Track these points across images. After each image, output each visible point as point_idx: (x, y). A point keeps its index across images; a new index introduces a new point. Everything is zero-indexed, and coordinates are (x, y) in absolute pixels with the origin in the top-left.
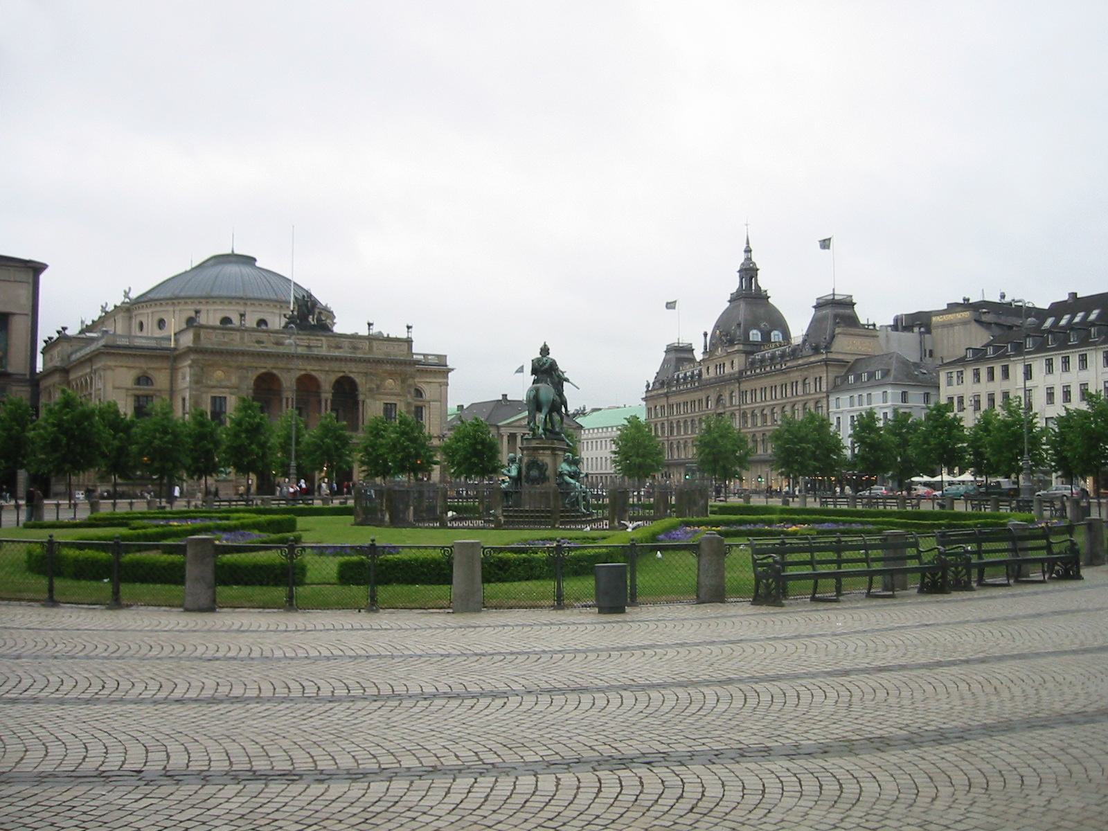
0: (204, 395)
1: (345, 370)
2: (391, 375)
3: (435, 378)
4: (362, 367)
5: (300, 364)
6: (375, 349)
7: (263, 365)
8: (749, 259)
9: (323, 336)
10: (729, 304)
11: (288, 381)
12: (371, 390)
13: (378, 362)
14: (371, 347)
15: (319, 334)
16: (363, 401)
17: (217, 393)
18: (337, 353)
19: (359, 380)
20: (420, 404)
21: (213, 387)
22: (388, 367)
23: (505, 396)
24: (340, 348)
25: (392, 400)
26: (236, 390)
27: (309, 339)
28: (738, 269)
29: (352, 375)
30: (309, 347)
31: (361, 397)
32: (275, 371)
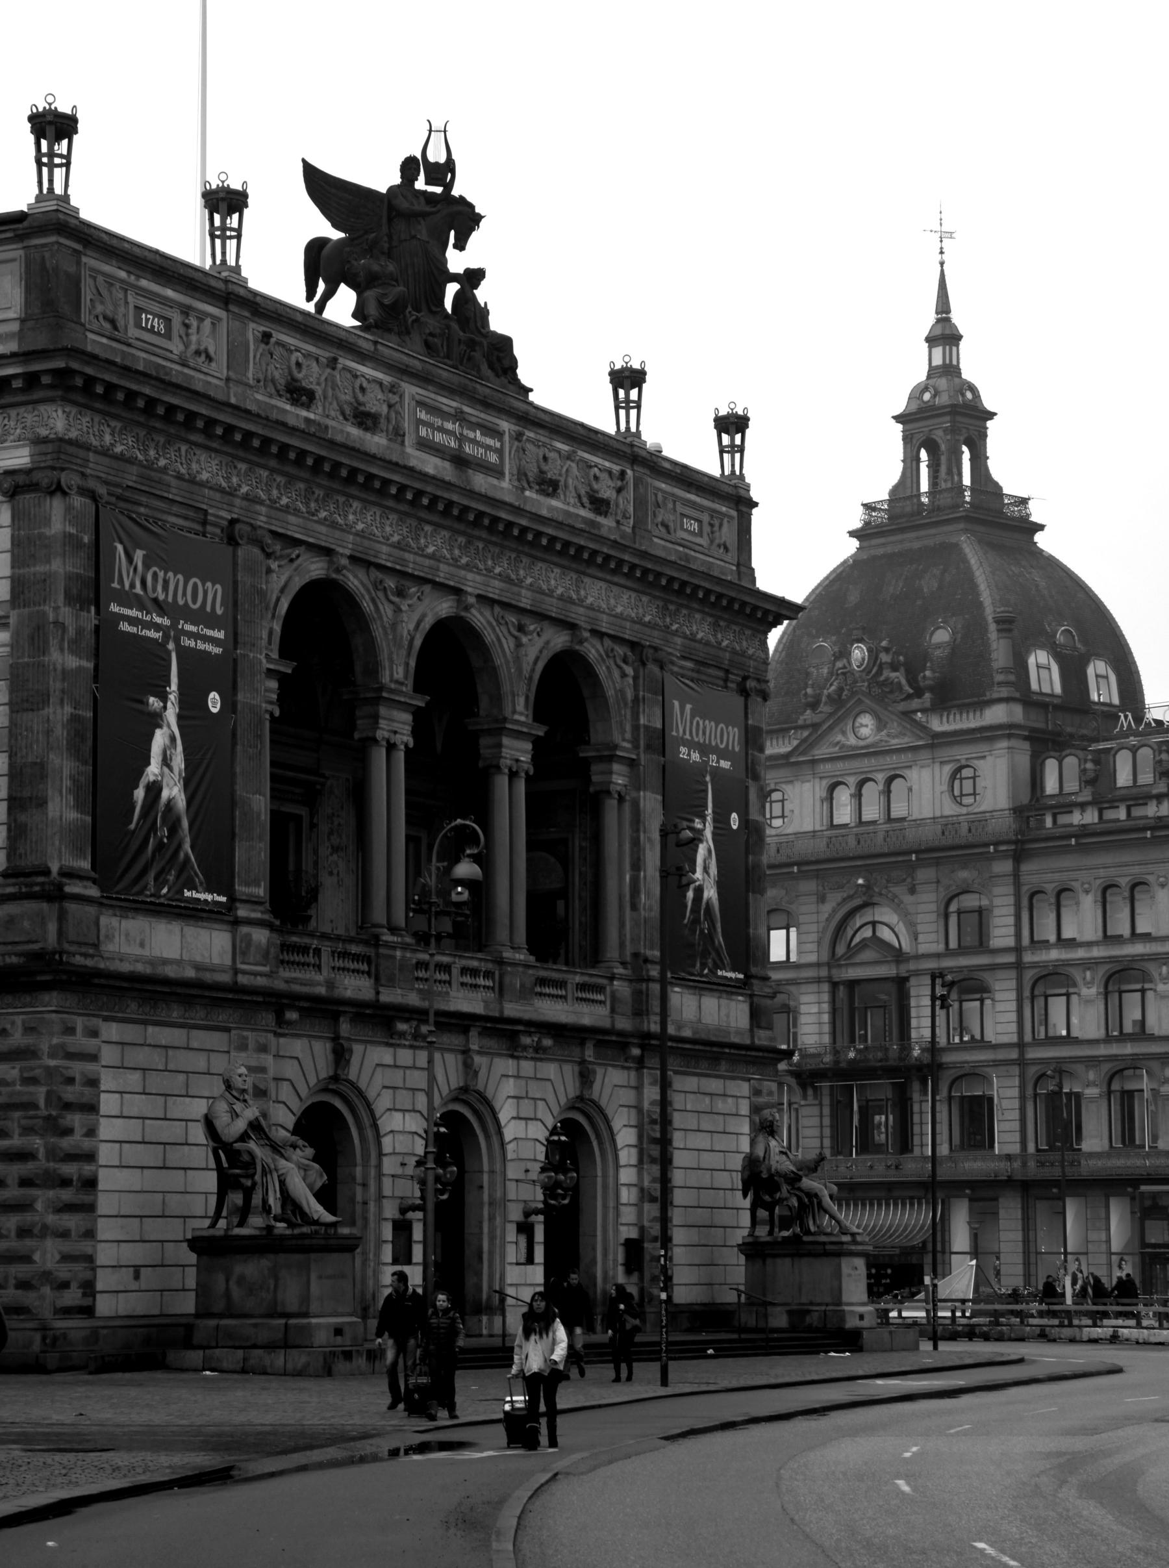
1: (578, 615)
7: (322, 535)
8: (950, 370)
10: (855, 544)
22: (701, 629)
24: (549, 487)
27: (459, 417)
28: (900, 407)
30: (460, 461)
32: (355, 581)
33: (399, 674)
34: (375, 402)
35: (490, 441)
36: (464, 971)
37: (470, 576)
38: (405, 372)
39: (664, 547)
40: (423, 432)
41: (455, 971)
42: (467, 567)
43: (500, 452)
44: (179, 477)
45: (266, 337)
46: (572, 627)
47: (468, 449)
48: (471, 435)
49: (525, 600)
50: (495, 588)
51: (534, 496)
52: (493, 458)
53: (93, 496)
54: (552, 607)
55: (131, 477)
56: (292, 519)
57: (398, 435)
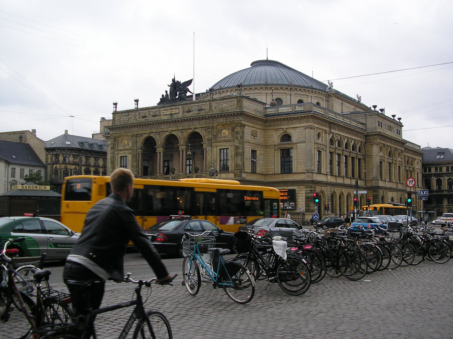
0: (116, 156)
2: (224, 126)
3: (300, 123)
4: (203, 123)
5: (164, 127)
6: (213, 108)
7: (145, 132)
9: (179, 105)
11: (160, 140)
12: (209, 140)
13: (213, 117)
14: (210, 107)
15: (177, 104)
16: (206, 149)
17: (122, 154)
18: (188, 115)
19: (202, 133)
20: (288, 146)
21: (121, 150)
22: (221, 120)
23: (34, 131)
24: (189, 111)
25: (224, 145)
26: (131, 151)
27: (171, 109)
29: (197, 131)
30: (171, 114)
31: (204, 146)
32: (152, 135)
33: (159, 143)
34: (157, 113)
35: (177, 110)
36: (172, 177)
37: (169, 129)
38: (161, 108)
39: (216, 111)
40: (164, 113)
41: (171, 177)
42: (169, 128)
43: (179, 111)
44: (124, 133)
45: (139, 113)
46: (192, 129)
47: (172, 113)
48: (173, 110)
49: (181, 128)
50: (174, 129)
51: (186, 113)
52: (177, 112)
53: (112, 138)
54: (186, 127)
55: (118, 135)
56: (140, 132)
57: (160, 115)
